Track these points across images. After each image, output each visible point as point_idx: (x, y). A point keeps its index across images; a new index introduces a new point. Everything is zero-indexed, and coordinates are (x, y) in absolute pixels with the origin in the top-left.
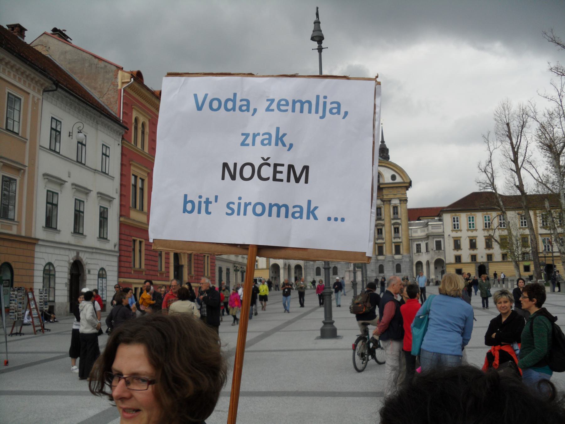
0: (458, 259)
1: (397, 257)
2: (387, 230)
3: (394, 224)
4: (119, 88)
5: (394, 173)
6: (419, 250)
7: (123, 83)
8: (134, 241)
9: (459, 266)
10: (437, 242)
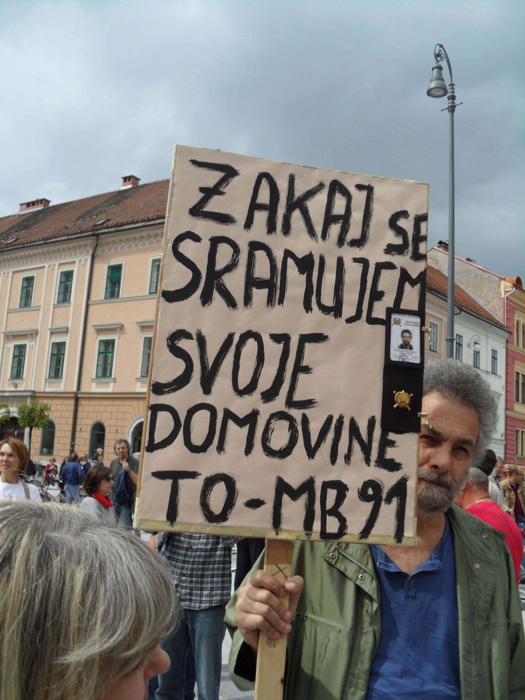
4: (503, 296)
7: (506, 292)
8: (517, 431)
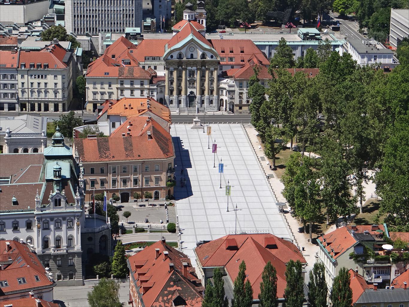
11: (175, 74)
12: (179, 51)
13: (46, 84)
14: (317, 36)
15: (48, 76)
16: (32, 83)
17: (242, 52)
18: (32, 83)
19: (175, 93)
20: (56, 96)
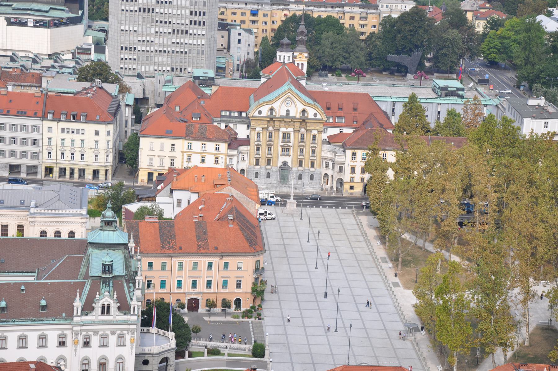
0: (352, 178)
1: (312, 169)
2: (307, 150)
3: (312, 147)
5: (316, 112)
6: (327, 166)
9: (352, 184)
10: (340, 167)
11: (264, 137)
12: (269, 106)
13: (83, 141)
14: (459, 92)
15: (246, 137)
16: (63, 140)
17: (355, 110)
18: (63, 140)
19: (263, 162)
20: (96, 159)
